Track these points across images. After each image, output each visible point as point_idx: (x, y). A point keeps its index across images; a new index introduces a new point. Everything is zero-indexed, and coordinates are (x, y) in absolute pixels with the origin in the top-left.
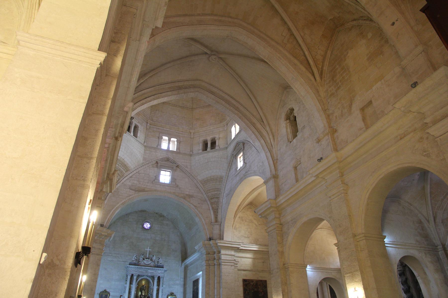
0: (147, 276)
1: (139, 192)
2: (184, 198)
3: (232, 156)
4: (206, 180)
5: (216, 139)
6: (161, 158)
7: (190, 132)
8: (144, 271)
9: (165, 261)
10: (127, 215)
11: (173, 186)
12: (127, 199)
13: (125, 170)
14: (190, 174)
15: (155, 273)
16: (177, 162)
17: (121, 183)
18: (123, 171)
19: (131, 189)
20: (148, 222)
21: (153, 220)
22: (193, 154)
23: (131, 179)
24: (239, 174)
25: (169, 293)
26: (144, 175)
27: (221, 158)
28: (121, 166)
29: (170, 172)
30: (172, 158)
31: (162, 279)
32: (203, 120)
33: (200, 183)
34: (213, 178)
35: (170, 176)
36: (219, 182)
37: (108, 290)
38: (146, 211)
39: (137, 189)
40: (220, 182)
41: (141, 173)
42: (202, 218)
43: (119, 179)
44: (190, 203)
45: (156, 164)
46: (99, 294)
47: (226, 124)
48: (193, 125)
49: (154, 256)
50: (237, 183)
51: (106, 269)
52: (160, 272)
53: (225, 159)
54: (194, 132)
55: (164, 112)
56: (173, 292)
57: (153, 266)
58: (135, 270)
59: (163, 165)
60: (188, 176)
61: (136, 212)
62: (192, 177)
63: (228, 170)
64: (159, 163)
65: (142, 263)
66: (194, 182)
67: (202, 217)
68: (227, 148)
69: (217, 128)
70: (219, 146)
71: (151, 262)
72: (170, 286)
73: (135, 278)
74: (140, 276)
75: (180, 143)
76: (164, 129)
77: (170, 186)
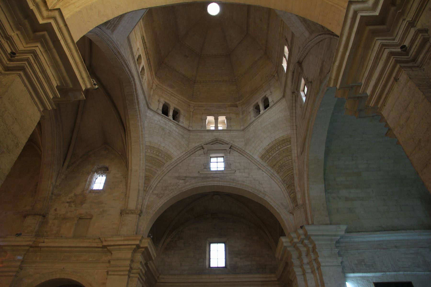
18: (288, 148)
28: (282, 146)
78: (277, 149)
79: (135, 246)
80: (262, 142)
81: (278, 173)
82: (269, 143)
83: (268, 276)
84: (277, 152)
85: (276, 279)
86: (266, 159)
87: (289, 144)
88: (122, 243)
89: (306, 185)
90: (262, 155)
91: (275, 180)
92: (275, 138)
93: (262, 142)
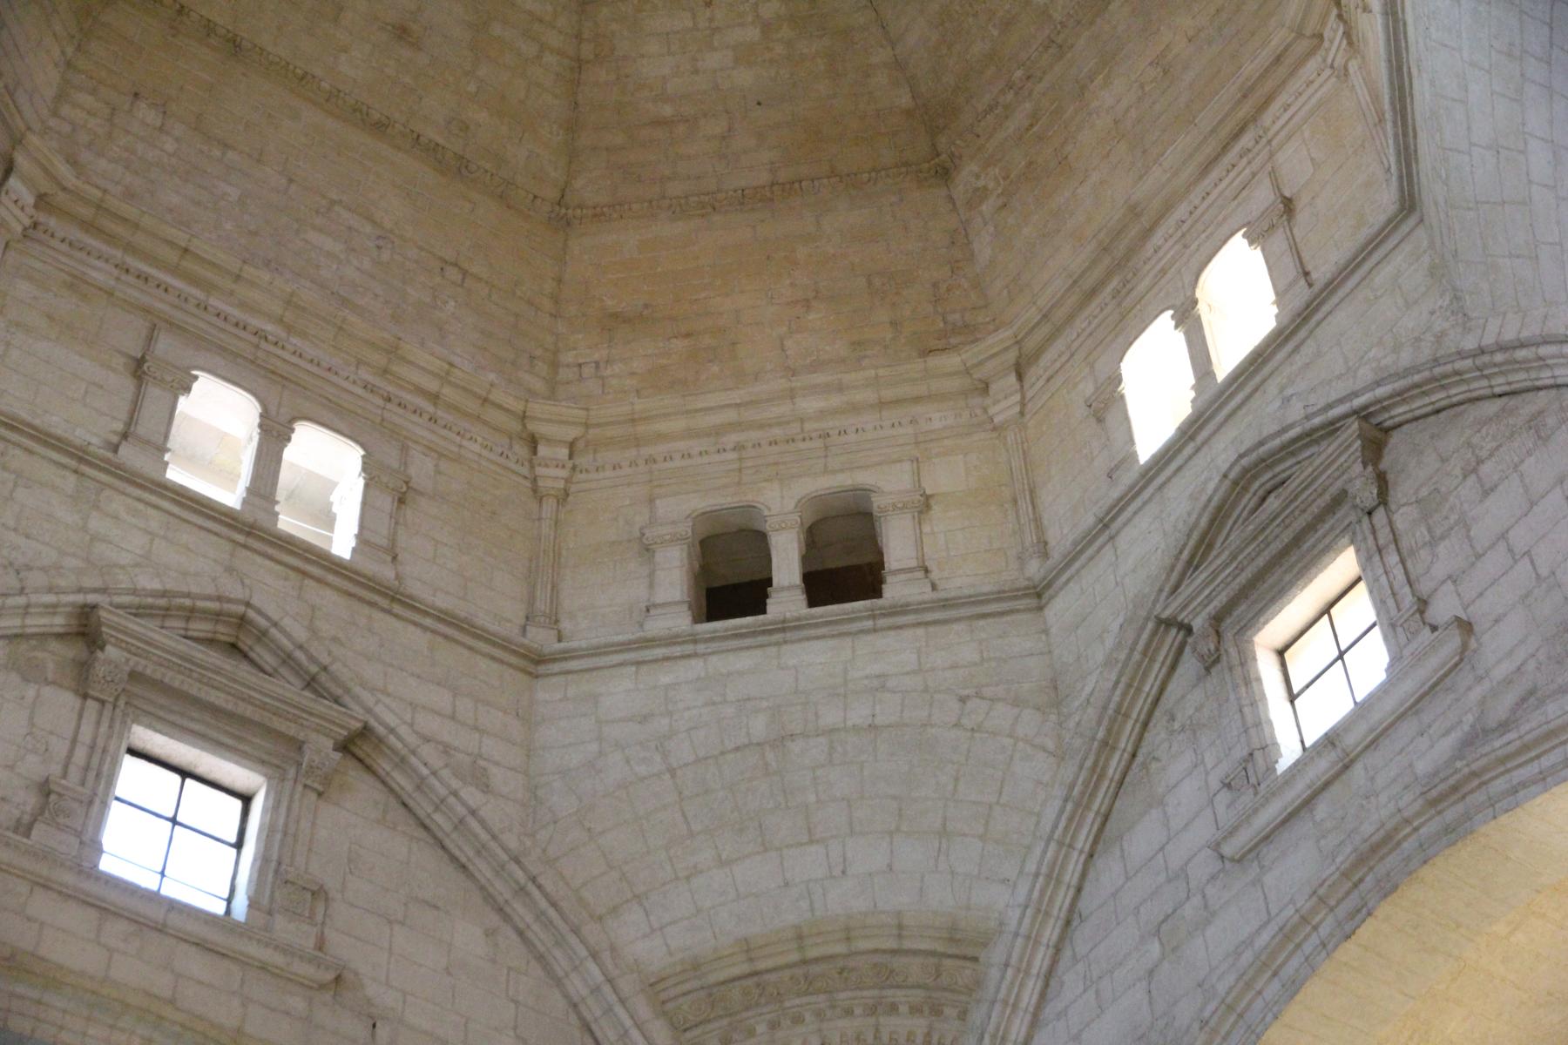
3: (1149, 652)
4: (736, 971)
5: (877, 502)
6: (148, 582)
7: (532, 427)
11: (278, 959)
14: (520, 875)
16: (357, 690)
22: (566, 656)
24: (1322, 809)
27: (963, 700)
29: (237, 804)
30: (301, 634)
32: (688, 335)
33: (644, 1010)
34: (840, 949)
35: (239, 845)
36: (915, 1010)
40: (937, 1011)
45: (73, 651)
47: (1012, 356)
48: (564, 374)
50: (1287, 935)
53: (1017, 702)
54: (571, 433)
55: (226, 146)
59: (176, 680)
60: (489, 898)
62: (540, 916)
63: (1083, 840)
64: (119, 644)
66: (559, 983)
68: (1039, 594)
69: (882, 405)
70: (927, 571)
75: (401, 501)
76: (215, 302)
77: (242, 961)
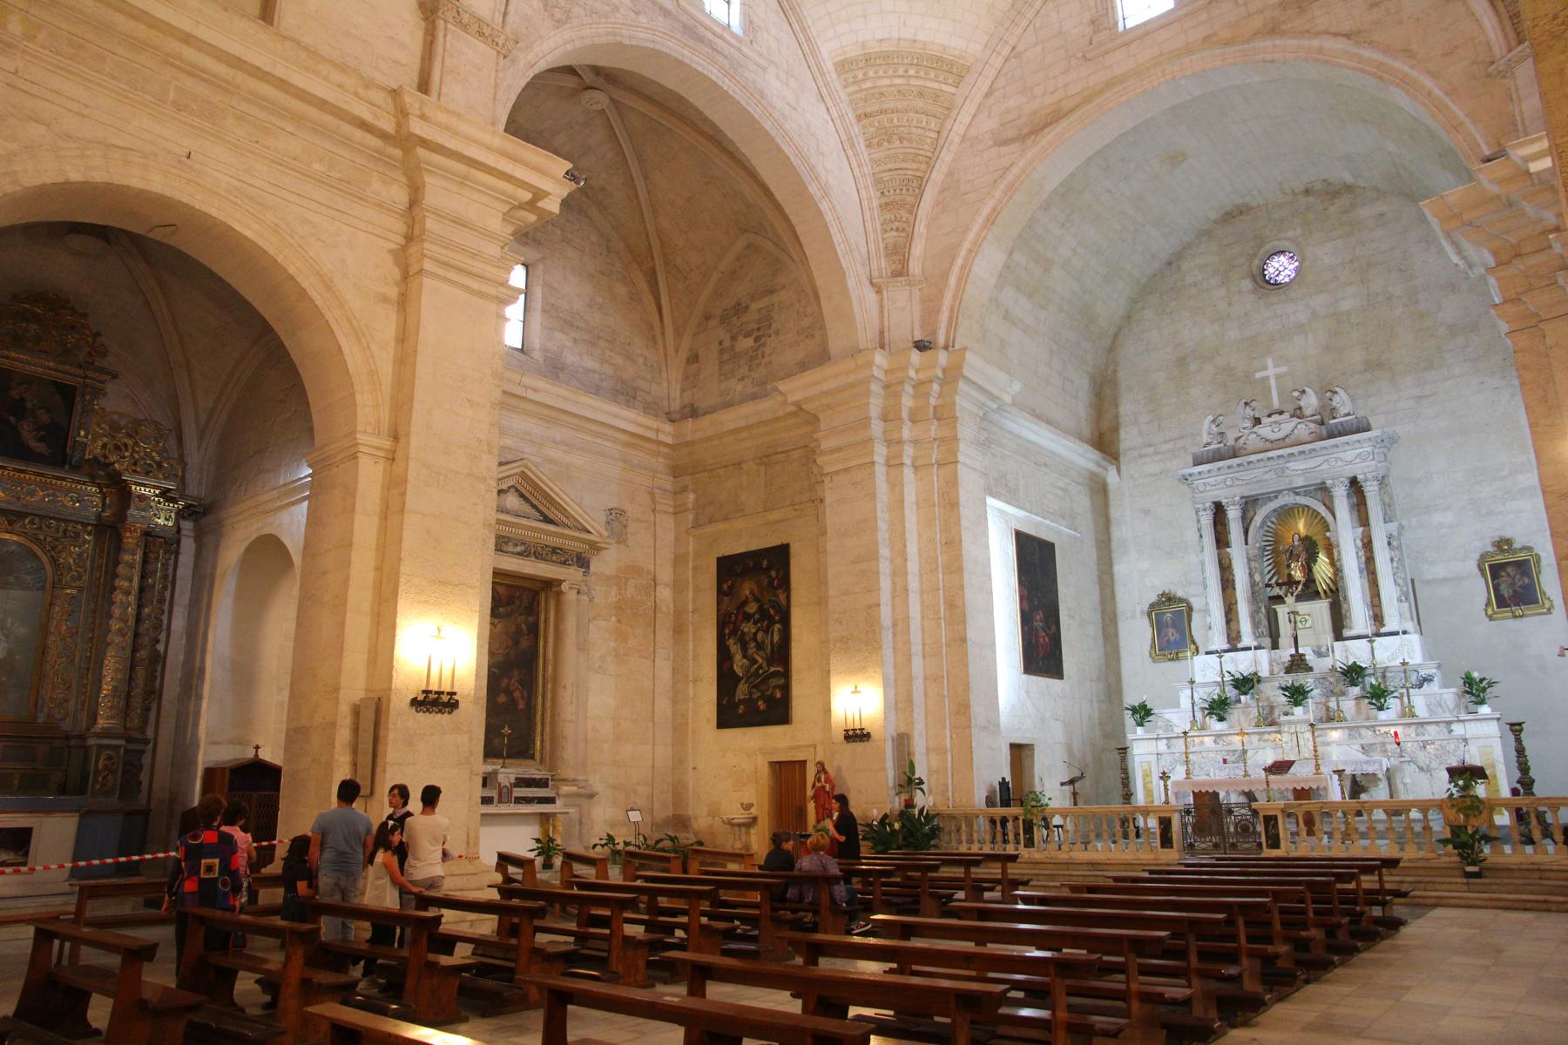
0: (1297, 494)
1: (1037, 135)
2: (1273, 30)
8: (1267, 472)
9: (1420, 397)
10: (1169, 264)
12: (998, 194)
13: (950, 81)
15: (1325, 466)
17: (957, 139)
19: (1006, 142)
20: (1283, 252)
21: (1299, 231)
23: (991, 100)
25: (1488, 542)
26: (1039, 49)
28: (922, 74)
31: (1372, 489)
37: (1180, 594)
38: (1252, 208)
39: (1026, 130)
41: (1025, 51)
42: (1414, 74)
43: (939, 132)
44: (1318, 34)
46: (1149, 615)
49: (1308, 390)
51: (1147, 512)
52: (1350, 455)
56: (1508, 534)
57: (1308, 439)
58: (1225, 481)
61: (1205, 234)
65: (1252, 441)
67: (1412, 67)
71: (1296, 420)
72: (1485, 511)
73: (1233, 514)
74: (1260, 502)
78: (901, 72)
79: (527, 196)
80: (865, 16)
81: (869, 146)
82: (888, 36)
83: (655, 424)
84: (898, 81)
85: (669, 440)
86: (851, 80)
87: (950, 81)
88: (490, 160)
89: (971, 236)
90: (843, 57)
91: (854, 164)
92: (915, 35)
93: (865, 16)
